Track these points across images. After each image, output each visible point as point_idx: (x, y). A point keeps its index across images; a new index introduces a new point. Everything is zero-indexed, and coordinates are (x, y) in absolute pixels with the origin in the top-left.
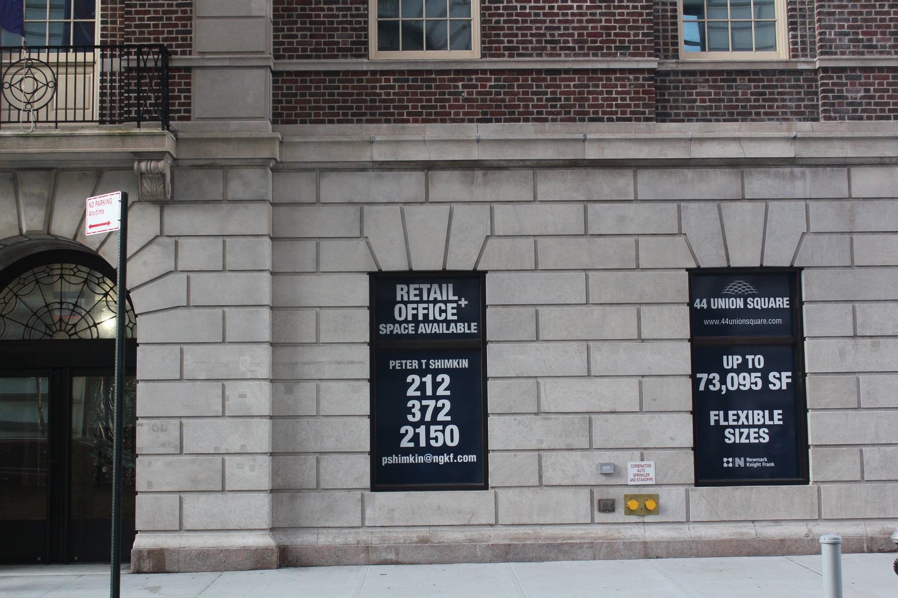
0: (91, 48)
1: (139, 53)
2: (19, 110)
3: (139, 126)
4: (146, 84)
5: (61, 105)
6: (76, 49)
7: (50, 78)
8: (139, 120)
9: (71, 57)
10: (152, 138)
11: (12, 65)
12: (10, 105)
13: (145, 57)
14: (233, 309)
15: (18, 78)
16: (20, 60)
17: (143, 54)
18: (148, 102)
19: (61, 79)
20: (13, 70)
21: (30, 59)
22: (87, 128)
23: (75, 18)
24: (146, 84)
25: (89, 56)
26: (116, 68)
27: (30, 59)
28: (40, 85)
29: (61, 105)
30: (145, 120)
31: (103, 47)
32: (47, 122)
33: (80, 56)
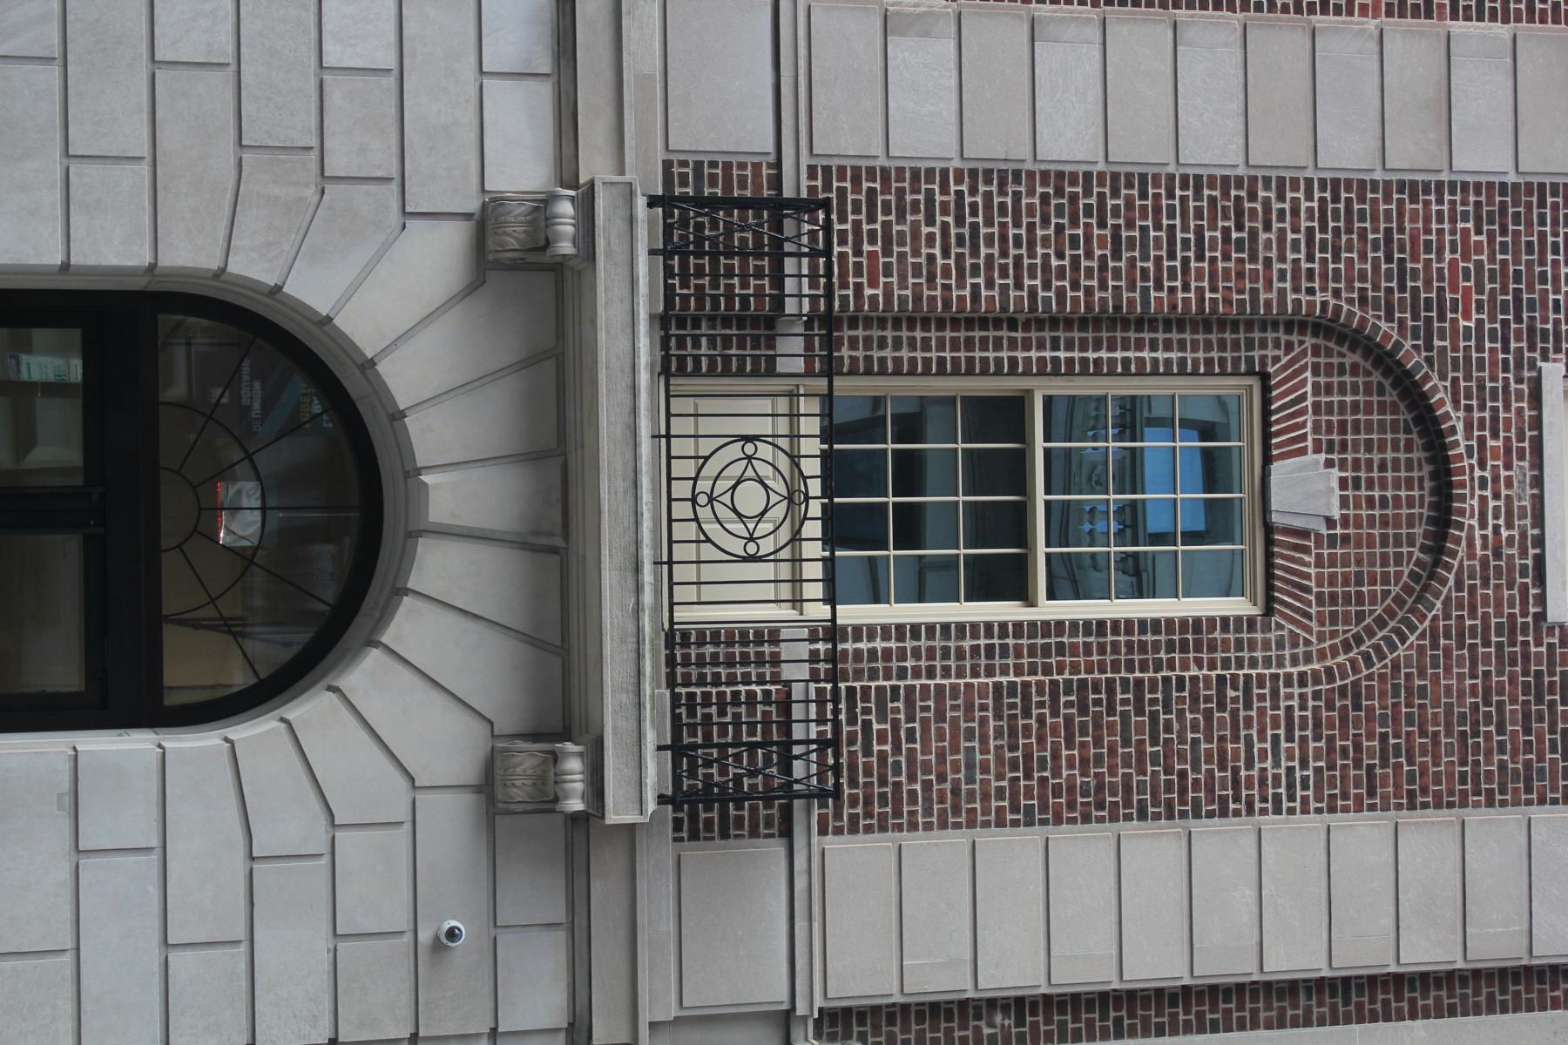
0: (831, 599)
1: (823, 743)
2: (695, 479)
3: (660, 748)
4: (743, 218)
5: (708, 573)
6: (825, 457)
7: (767, 546)
8: (677, 749)
9: (811, 446)
10: (636, 784)
11: (794, 459)
12: (706, 459)
13: (814, 756)
14: (243, 966)
15: (765, 471)
16: (805, 478)
17: (821, 752)
18: (716, 778)
19: (765, 570)
20: (783, 463)
21: (807, 498)
22: (657, 592)
23: (894, 504)
24: (743, 218)
25: (815, 590)
26: (787, 672)
27: (807, 498)
28: (751, 526)
29: (708, 573)
30: (667, 215)
31: (833, 632)
32: (671, 542)
33: (814, 570)
